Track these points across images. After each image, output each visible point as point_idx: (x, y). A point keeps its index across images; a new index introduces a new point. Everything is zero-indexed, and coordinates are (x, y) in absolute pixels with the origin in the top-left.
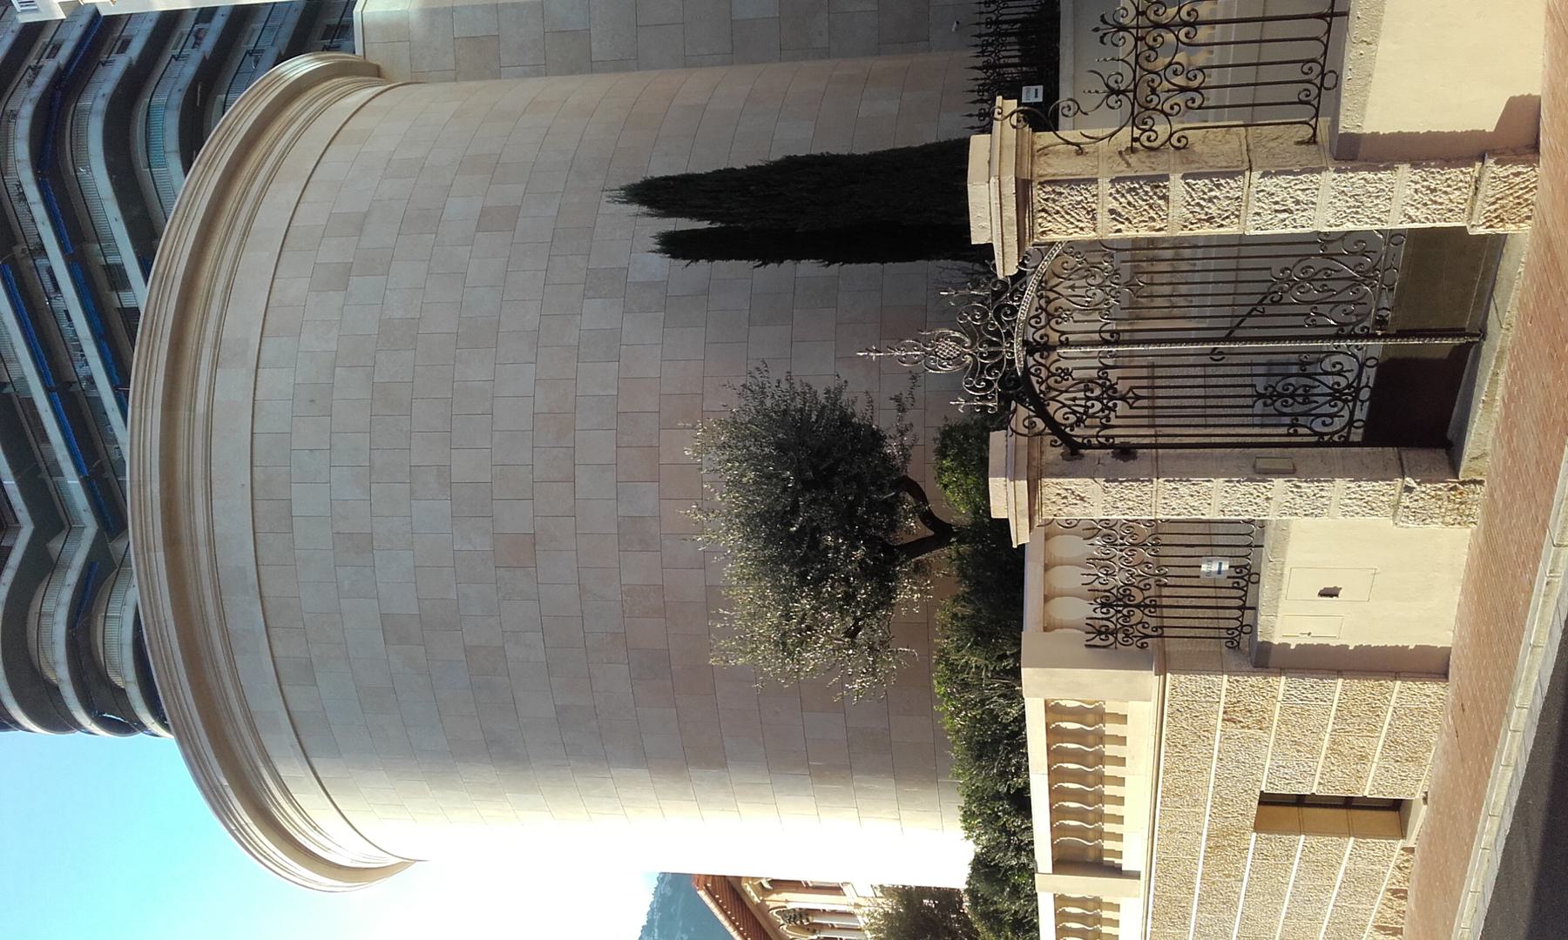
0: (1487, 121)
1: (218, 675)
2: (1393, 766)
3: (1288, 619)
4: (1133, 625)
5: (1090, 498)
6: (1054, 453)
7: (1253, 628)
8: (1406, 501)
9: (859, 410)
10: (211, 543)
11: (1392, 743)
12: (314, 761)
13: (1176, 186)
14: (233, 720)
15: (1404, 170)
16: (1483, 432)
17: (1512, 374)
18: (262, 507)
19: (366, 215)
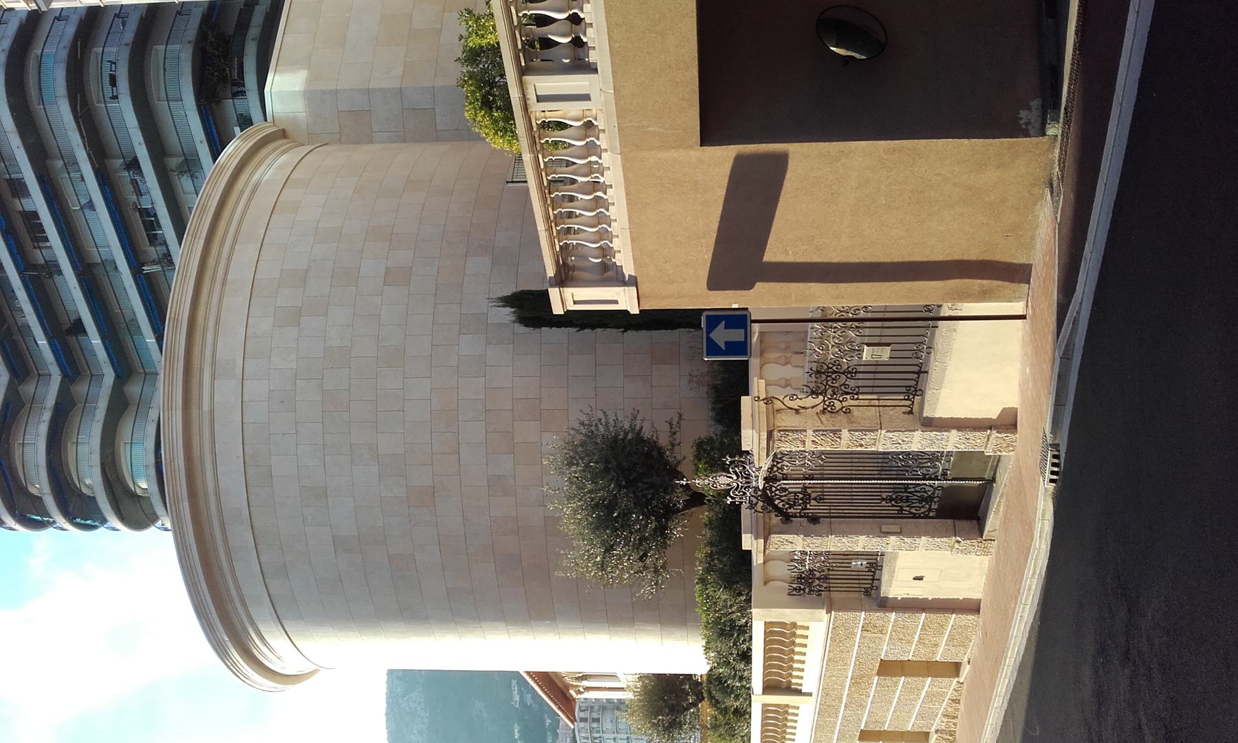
0: (993, 413)
1: (223, 576)
2: (953, 649)
3: (896, 586)
4: (811, 585)
5: (796, 543)
6: (776, 520)
7: (878, 588)
8: (957, 545)
9: (646, 433)
10: (217, 494)
11: (951, 638)
12: (284, 622)
13: (845, 434)
14: (232, 601)
15: (954, 432)
16: (993, 522)
17: (1007, 506)
18: (250, 471)
19: (307, 271)
